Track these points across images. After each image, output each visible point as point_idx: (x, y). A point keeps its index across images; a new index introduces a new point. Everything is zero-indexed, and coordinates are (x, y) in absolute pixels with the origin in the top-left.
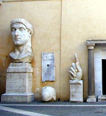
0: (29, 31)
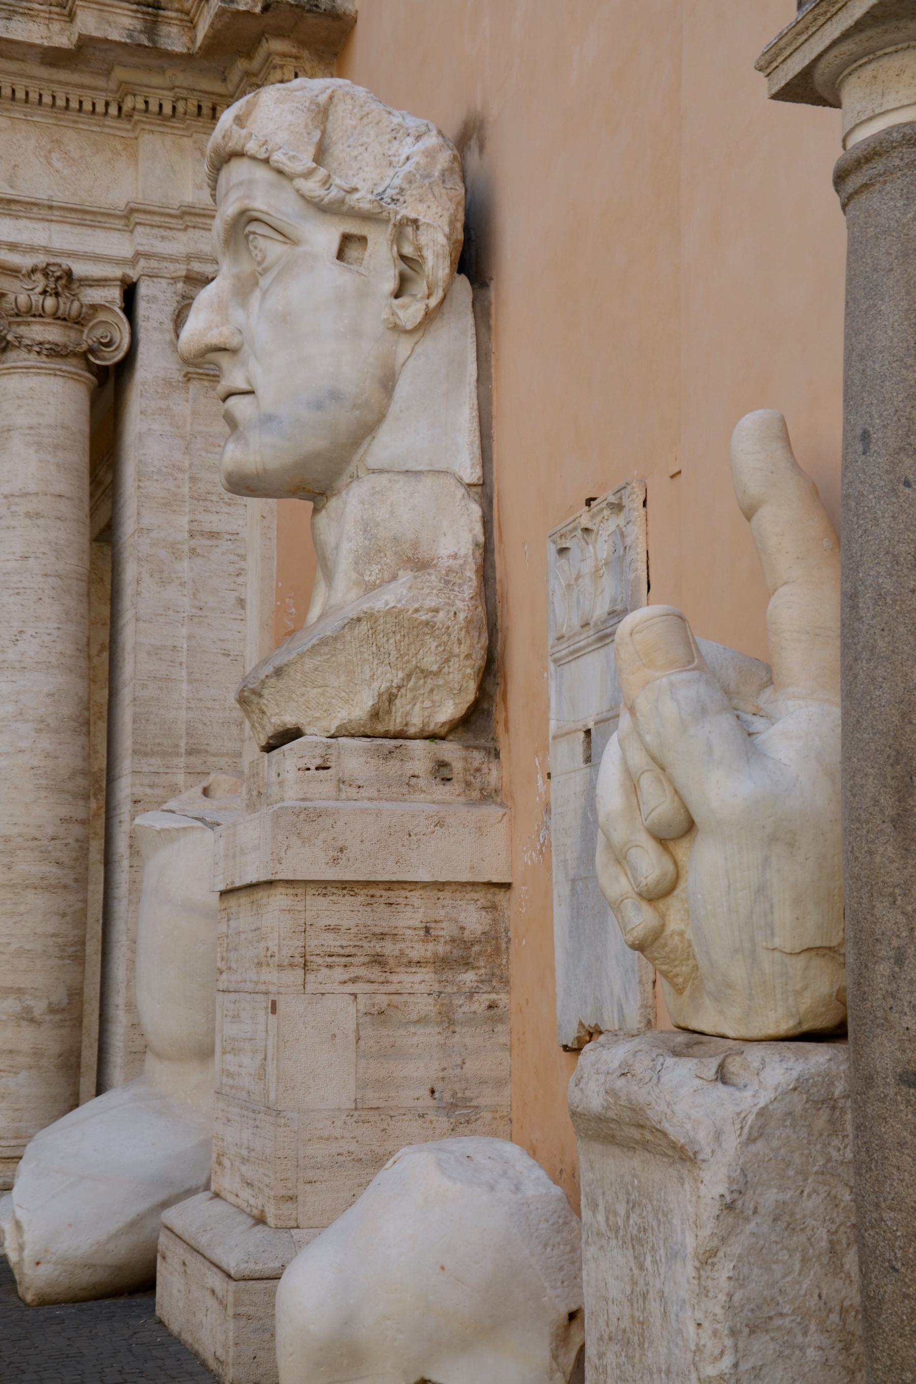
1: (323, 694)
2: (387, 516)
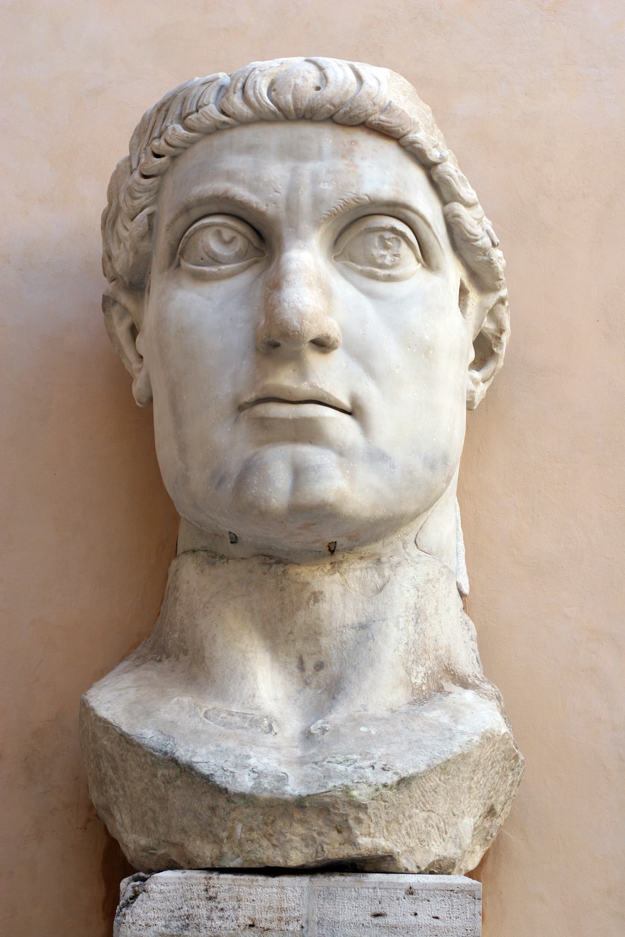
0: (474, 297)
1: (426, 821)
2: (433, 612)
